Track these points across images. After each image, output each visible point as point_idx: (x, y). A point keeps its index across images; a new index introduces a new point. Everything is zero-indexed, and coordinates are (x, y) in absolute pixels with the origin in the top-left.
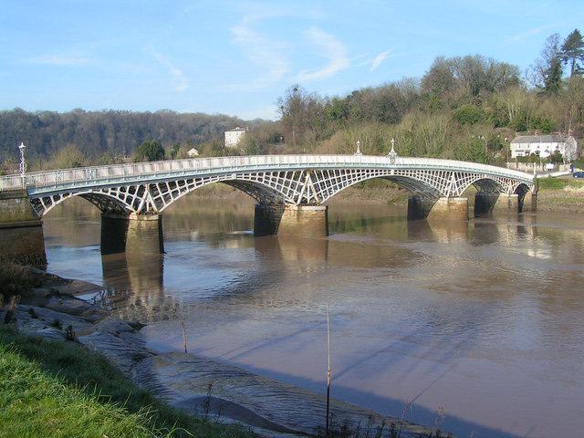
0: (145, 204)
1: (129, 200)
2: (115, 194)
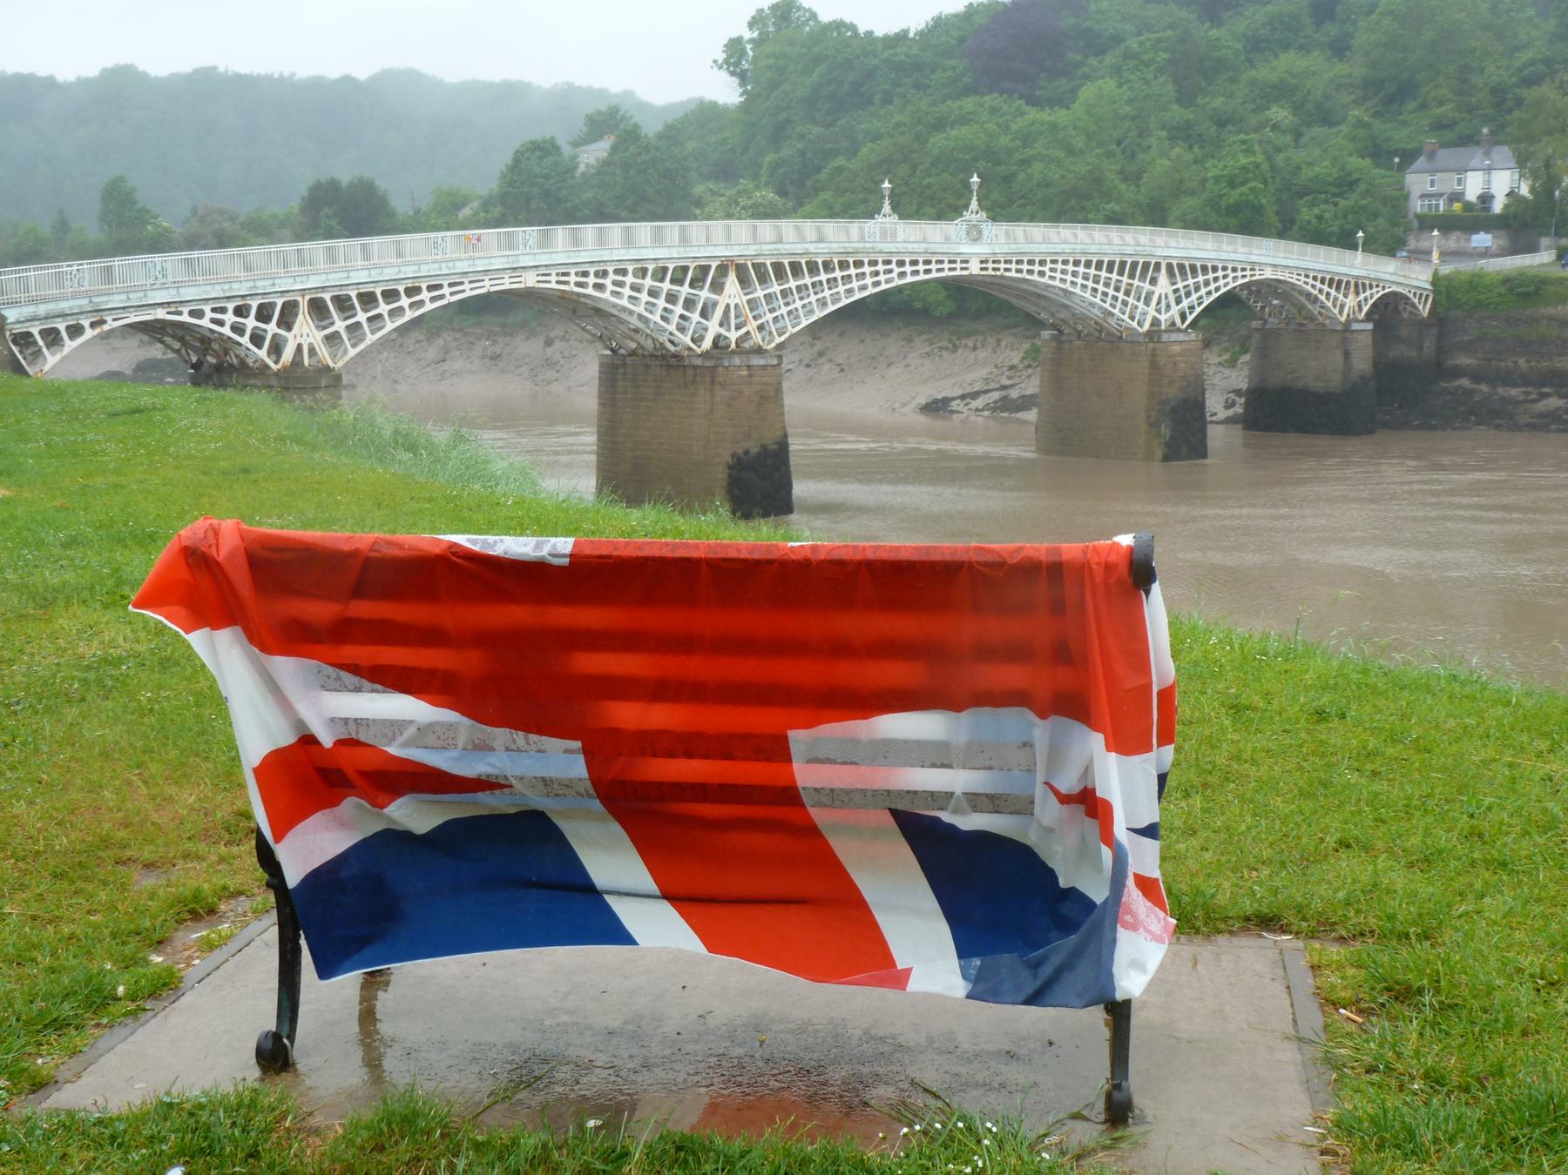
0: (299, 348)
1: (257, 339)
2: (221, 323)
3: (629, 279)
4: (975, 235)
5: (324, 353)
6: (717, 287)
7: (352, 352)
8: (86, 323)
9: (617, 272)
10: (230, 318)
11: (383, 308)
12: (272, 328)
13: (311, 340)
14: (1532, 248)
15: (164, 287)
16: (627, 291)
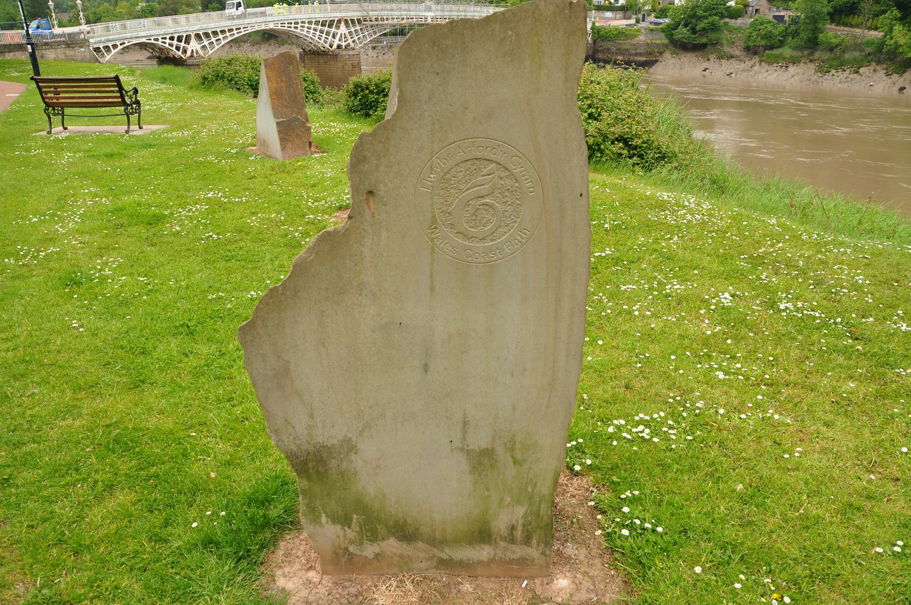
0: (192, 51)
1: (178, 48)
2: (165, 43)
3: (306, 25)
4: (429, 9)
5: (201, 53)
6: (338, 27)
7: (211, 52)
8: (118, 44)
9: (302, 22)
10: (168, 41)
11: (221, 36)
12: (182, 44)
13: (196, 48)
14: (630, 18)
15: (144, 30)
16: (306, 29)
